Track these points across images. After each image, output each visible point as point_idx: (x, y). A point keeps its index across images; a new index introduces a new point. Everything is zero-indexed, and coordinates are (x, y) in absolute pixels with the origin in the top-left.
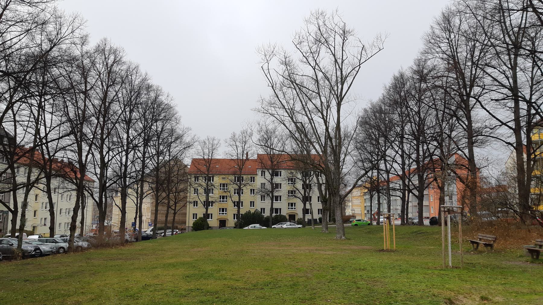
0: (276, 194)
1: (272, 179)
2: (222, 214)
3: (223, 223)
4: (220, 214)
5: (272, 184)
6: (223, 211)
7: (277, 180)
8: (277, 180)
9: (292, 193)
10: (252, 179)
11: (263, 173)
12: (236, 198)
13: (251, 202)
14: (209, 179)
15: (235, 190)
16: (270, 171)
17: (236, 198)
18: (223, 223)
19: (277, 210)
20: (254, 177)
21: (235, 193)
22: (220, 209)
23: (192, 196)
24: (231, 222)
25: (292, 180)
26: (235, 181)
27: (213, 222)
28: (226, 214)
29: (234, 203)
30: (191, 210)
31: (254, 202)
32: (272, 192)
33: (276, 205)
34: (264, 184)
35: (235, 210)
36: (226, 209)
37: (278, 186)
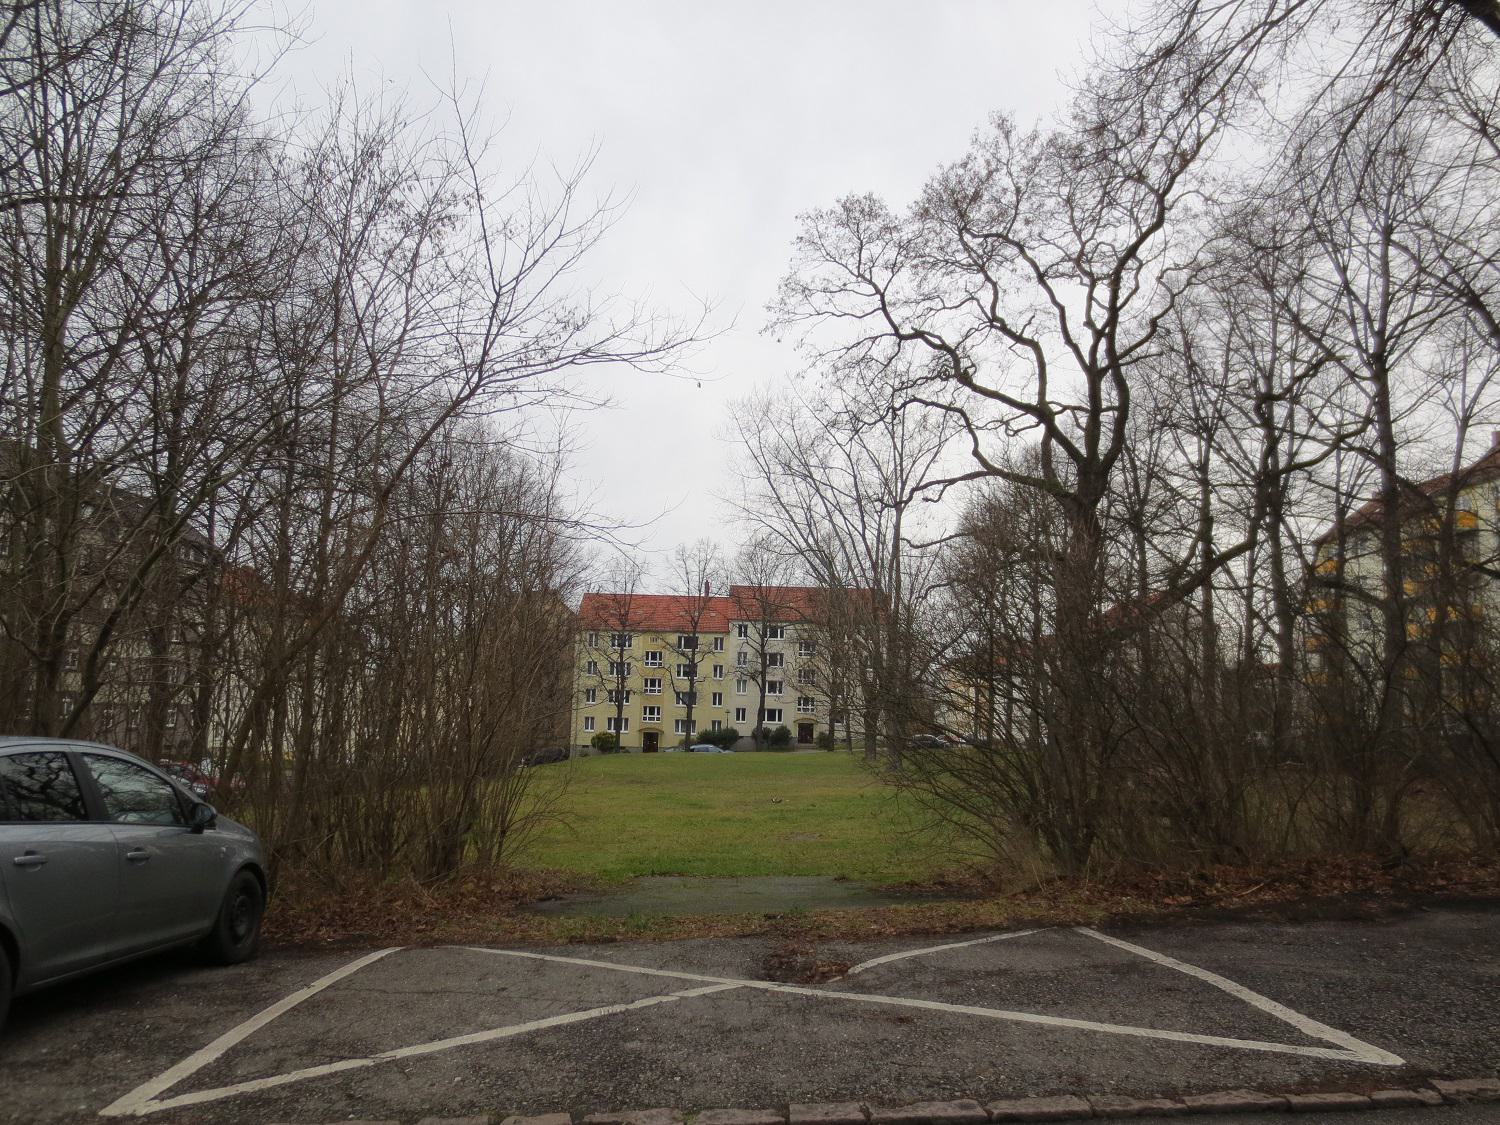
0: (769, 678)
1: (763, 646)
2: (650, 719)
3: (651, 741)
4: (645, 719)
5: (763, 655)
6: (652, 712)
7: (775, 645)
8: (775, 645)
9: (807, 675)
10: (719, 644)
11: (743, 631)
12: (683, 684)
13: (715, 695)
14: (622, 642)
15: (679, 666)
16: (760, 626)
17: (683, 684)
18: (651, 741)
19: (772, 715)
20: (722, 640)
21: (679, 675)
22: (645, 708)
23: (585, 681)
24: (672, 736)
25: (808, 645)
26: (680, 647)
27: (630, 737)
28: (658, 719)
29: (678, 694)
30: (583, 709)
31: (720, 695)
32: (763, 673)
33: (771, 701)
34: (746, 654)
35: (680, 711)
36: (659, 709)
37: (775, 659)
